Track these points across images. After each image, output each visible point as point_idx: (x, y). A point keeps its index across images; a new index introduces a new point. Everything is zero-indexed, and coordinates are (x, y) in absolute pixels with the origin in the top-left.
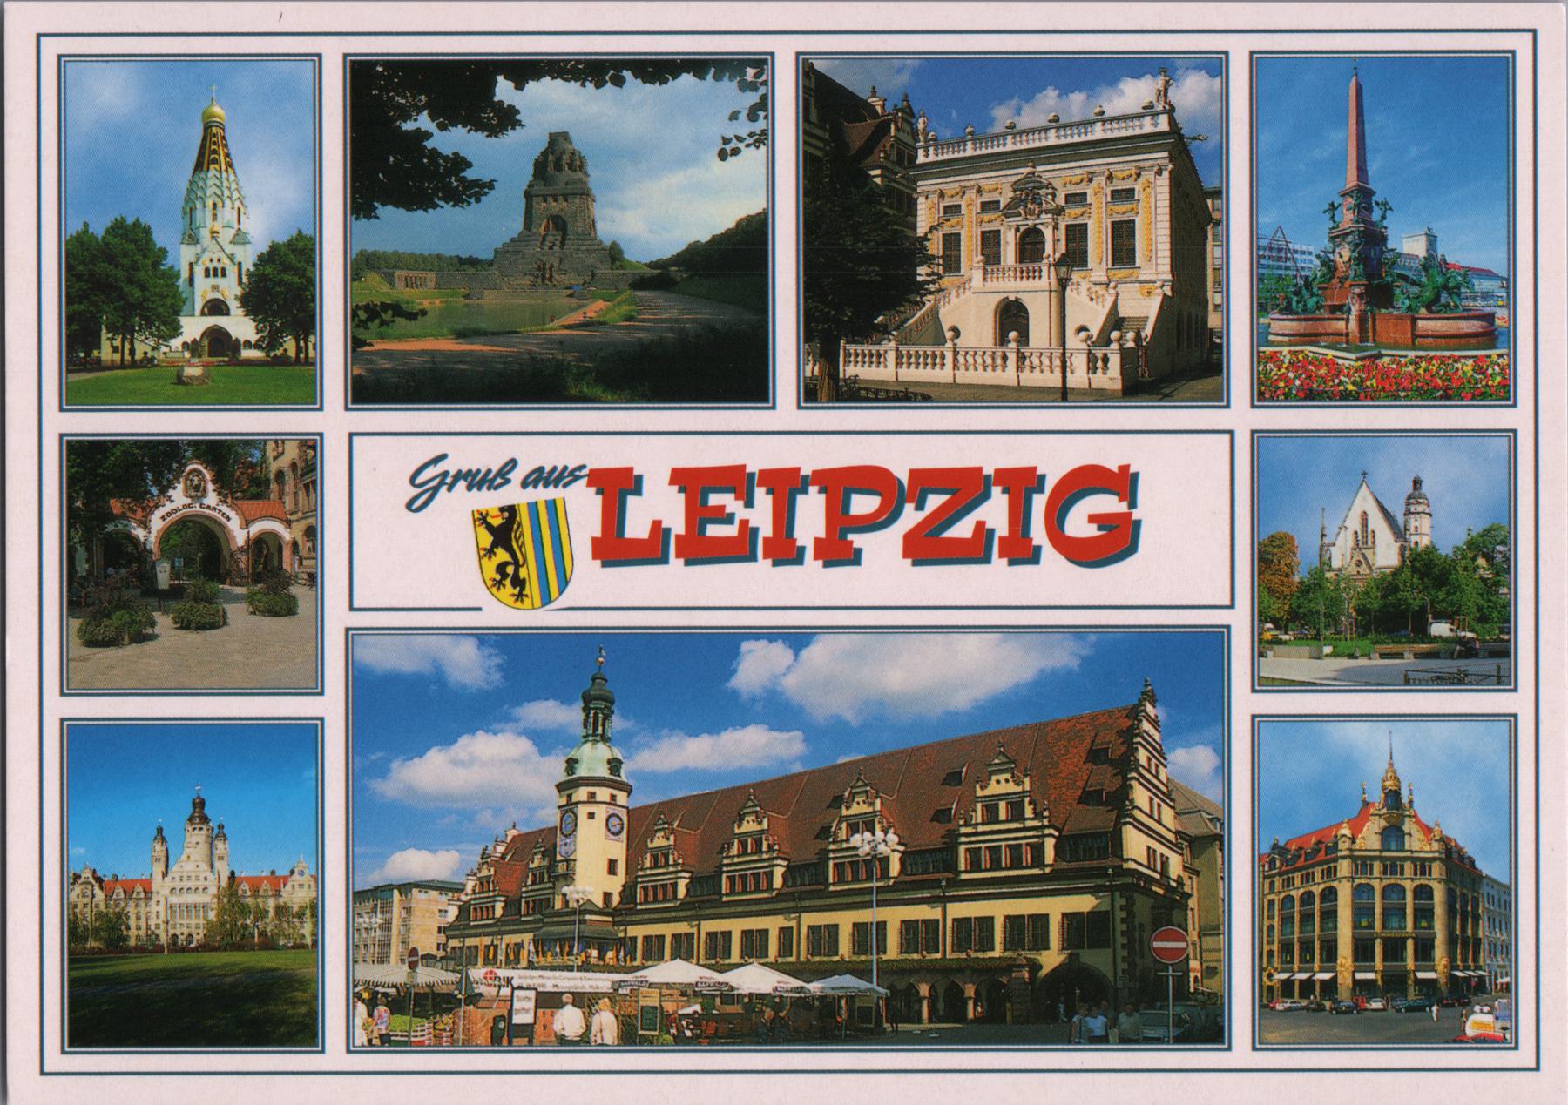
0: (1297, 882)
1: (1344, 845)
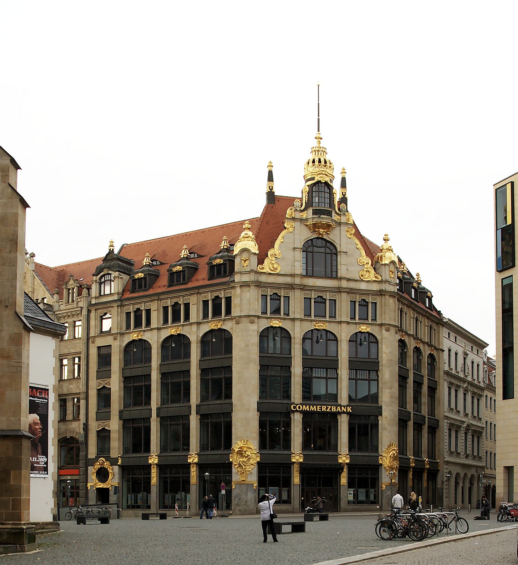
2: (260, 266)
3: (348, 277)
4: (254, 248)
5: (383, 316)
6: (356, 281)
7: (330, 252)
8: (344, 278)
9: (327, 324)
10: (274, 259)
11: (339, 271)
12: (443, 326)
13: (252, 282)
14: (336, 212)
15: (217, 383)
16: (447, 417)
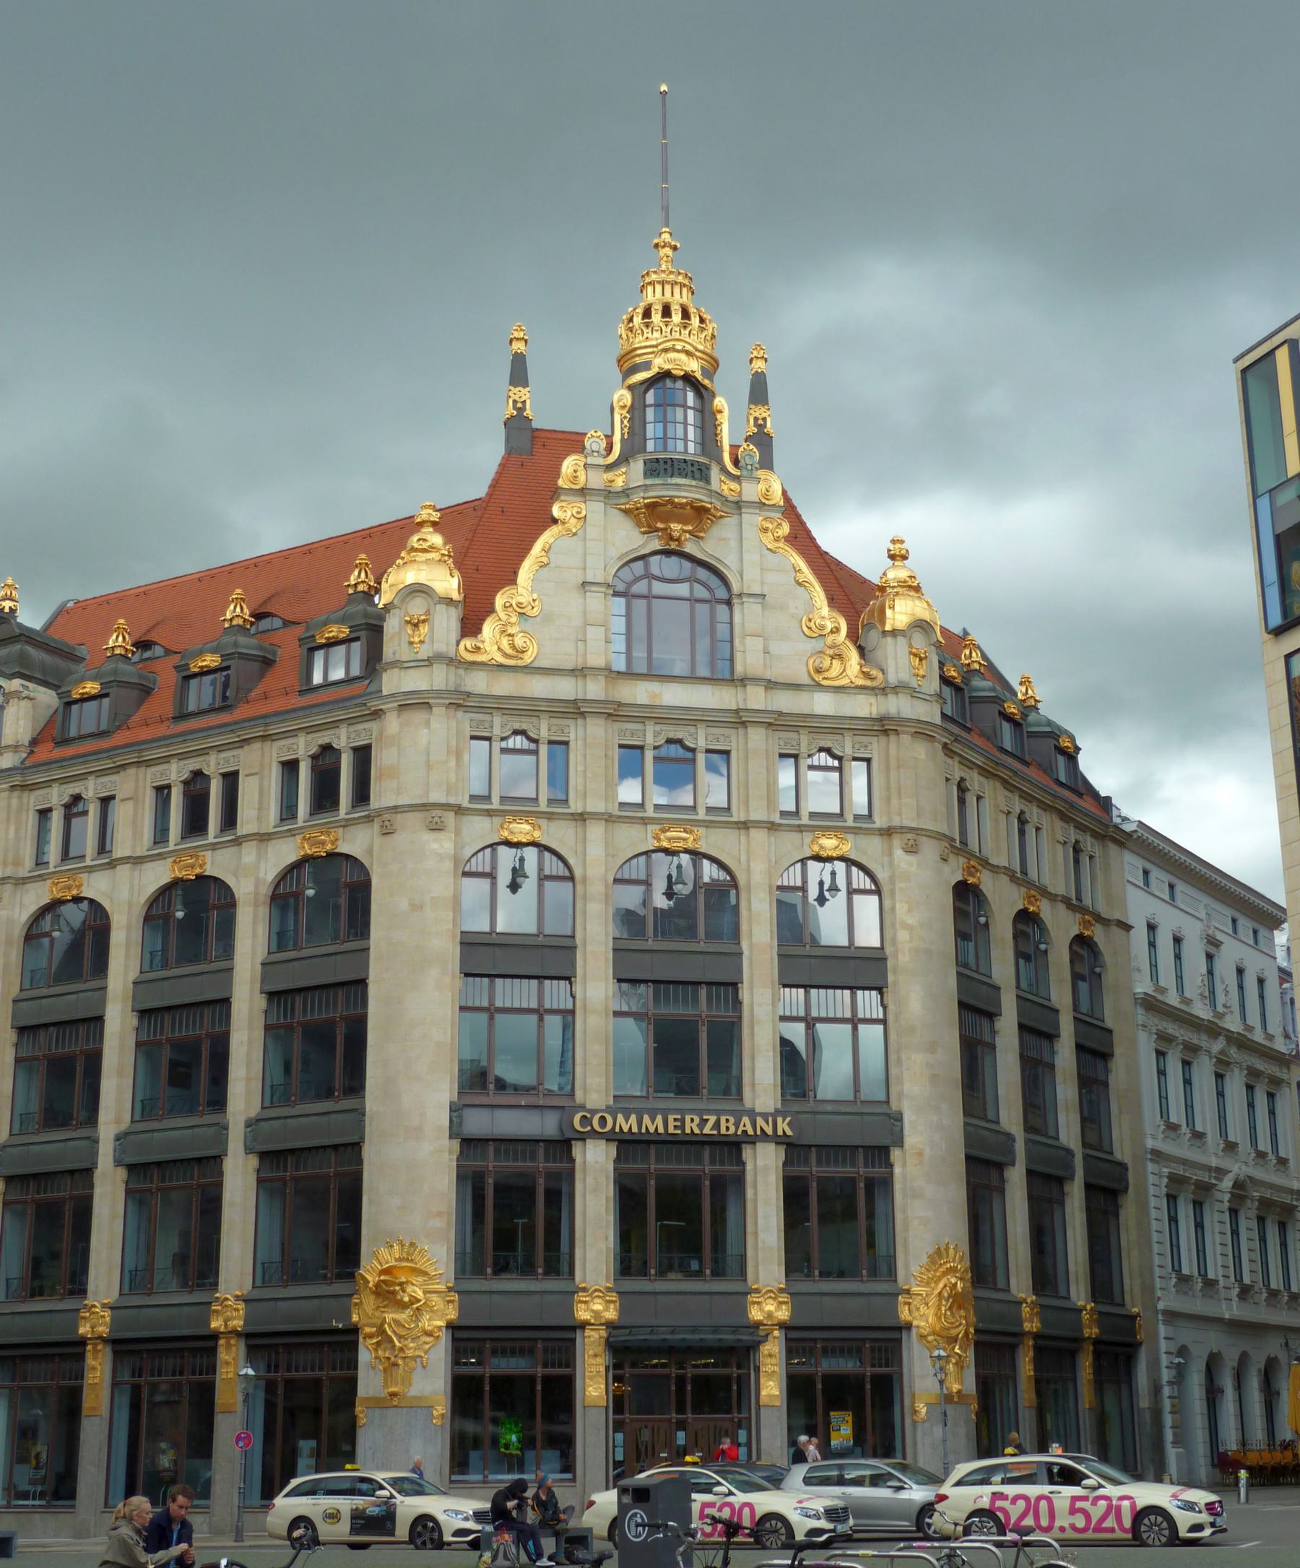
0: (132, 826)
1: (421, 641)
2: (468, 643)
3: (768, 675)
4: (448, 583)
5: (895, 802)
6: (797, 687)
7: (704, 594)
8: (756, 680)
9: (701, 831)
10: (514, 619)
11: (738, 657)
12: (1121, 844)
13: (439, 693)
14: (724, 470)
15: (319, 1036)
16: (1157, 1155)
